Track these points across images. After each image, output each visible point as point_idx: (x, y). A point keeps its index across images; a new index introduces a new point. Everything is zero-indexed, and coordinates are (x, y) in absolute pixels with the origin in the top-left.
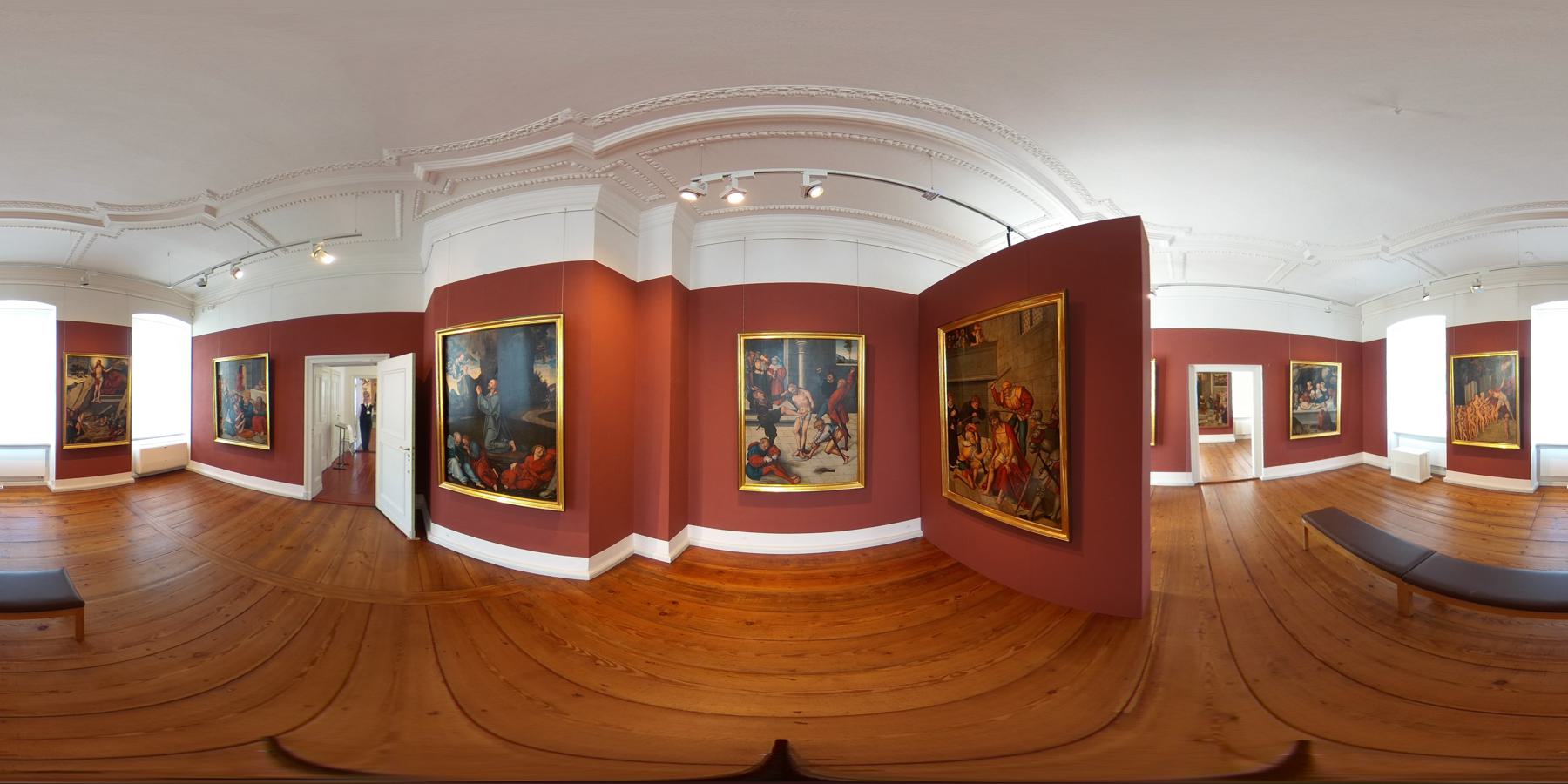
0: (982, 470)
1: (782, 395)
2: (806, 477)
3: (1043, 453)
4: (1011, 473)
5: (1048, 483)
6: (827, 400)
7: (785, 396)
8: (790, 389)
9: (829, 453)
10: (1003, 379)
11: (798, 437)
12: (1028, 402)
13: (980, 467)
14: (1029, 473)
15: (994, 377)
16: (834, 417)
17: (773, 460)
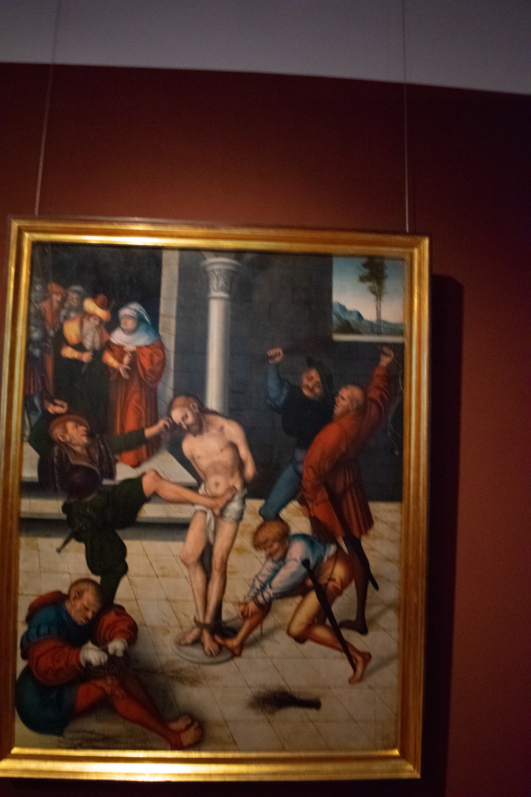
1: (149, 432)
2: (225, 723)
6: (299, 455)
7: (157, 438)
8: (177, 415)
9: (300, 639)
11: (199, 577)
16: (320, 511)
17: (112, 658)
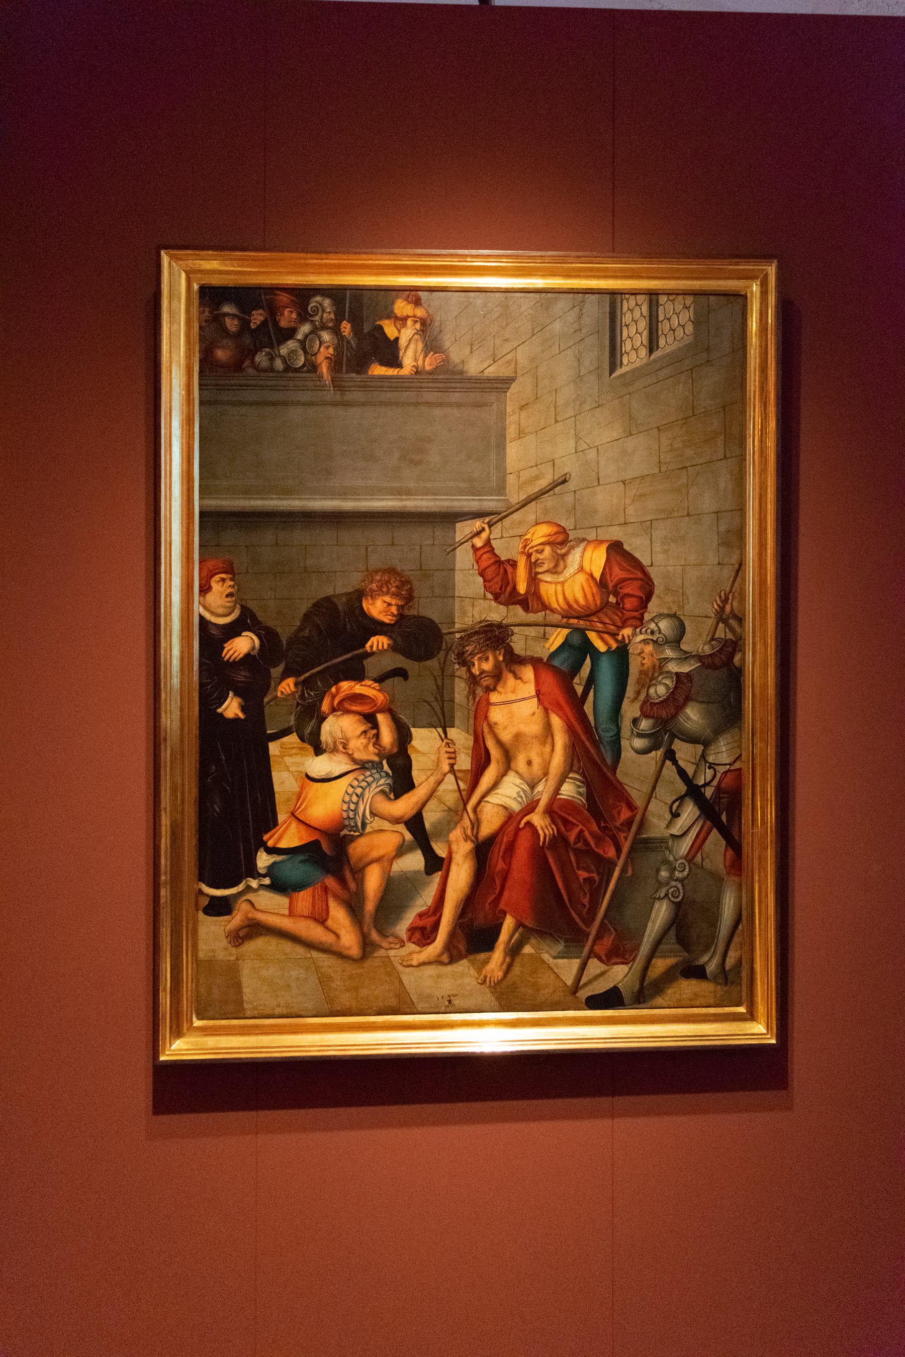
0: (415, 861)
3: (685, 752)
4: (558, 842)
5: (698, 845)
10: (530, 513)
13: (402, 851)
14: (629, 823)
15: (490, 503)
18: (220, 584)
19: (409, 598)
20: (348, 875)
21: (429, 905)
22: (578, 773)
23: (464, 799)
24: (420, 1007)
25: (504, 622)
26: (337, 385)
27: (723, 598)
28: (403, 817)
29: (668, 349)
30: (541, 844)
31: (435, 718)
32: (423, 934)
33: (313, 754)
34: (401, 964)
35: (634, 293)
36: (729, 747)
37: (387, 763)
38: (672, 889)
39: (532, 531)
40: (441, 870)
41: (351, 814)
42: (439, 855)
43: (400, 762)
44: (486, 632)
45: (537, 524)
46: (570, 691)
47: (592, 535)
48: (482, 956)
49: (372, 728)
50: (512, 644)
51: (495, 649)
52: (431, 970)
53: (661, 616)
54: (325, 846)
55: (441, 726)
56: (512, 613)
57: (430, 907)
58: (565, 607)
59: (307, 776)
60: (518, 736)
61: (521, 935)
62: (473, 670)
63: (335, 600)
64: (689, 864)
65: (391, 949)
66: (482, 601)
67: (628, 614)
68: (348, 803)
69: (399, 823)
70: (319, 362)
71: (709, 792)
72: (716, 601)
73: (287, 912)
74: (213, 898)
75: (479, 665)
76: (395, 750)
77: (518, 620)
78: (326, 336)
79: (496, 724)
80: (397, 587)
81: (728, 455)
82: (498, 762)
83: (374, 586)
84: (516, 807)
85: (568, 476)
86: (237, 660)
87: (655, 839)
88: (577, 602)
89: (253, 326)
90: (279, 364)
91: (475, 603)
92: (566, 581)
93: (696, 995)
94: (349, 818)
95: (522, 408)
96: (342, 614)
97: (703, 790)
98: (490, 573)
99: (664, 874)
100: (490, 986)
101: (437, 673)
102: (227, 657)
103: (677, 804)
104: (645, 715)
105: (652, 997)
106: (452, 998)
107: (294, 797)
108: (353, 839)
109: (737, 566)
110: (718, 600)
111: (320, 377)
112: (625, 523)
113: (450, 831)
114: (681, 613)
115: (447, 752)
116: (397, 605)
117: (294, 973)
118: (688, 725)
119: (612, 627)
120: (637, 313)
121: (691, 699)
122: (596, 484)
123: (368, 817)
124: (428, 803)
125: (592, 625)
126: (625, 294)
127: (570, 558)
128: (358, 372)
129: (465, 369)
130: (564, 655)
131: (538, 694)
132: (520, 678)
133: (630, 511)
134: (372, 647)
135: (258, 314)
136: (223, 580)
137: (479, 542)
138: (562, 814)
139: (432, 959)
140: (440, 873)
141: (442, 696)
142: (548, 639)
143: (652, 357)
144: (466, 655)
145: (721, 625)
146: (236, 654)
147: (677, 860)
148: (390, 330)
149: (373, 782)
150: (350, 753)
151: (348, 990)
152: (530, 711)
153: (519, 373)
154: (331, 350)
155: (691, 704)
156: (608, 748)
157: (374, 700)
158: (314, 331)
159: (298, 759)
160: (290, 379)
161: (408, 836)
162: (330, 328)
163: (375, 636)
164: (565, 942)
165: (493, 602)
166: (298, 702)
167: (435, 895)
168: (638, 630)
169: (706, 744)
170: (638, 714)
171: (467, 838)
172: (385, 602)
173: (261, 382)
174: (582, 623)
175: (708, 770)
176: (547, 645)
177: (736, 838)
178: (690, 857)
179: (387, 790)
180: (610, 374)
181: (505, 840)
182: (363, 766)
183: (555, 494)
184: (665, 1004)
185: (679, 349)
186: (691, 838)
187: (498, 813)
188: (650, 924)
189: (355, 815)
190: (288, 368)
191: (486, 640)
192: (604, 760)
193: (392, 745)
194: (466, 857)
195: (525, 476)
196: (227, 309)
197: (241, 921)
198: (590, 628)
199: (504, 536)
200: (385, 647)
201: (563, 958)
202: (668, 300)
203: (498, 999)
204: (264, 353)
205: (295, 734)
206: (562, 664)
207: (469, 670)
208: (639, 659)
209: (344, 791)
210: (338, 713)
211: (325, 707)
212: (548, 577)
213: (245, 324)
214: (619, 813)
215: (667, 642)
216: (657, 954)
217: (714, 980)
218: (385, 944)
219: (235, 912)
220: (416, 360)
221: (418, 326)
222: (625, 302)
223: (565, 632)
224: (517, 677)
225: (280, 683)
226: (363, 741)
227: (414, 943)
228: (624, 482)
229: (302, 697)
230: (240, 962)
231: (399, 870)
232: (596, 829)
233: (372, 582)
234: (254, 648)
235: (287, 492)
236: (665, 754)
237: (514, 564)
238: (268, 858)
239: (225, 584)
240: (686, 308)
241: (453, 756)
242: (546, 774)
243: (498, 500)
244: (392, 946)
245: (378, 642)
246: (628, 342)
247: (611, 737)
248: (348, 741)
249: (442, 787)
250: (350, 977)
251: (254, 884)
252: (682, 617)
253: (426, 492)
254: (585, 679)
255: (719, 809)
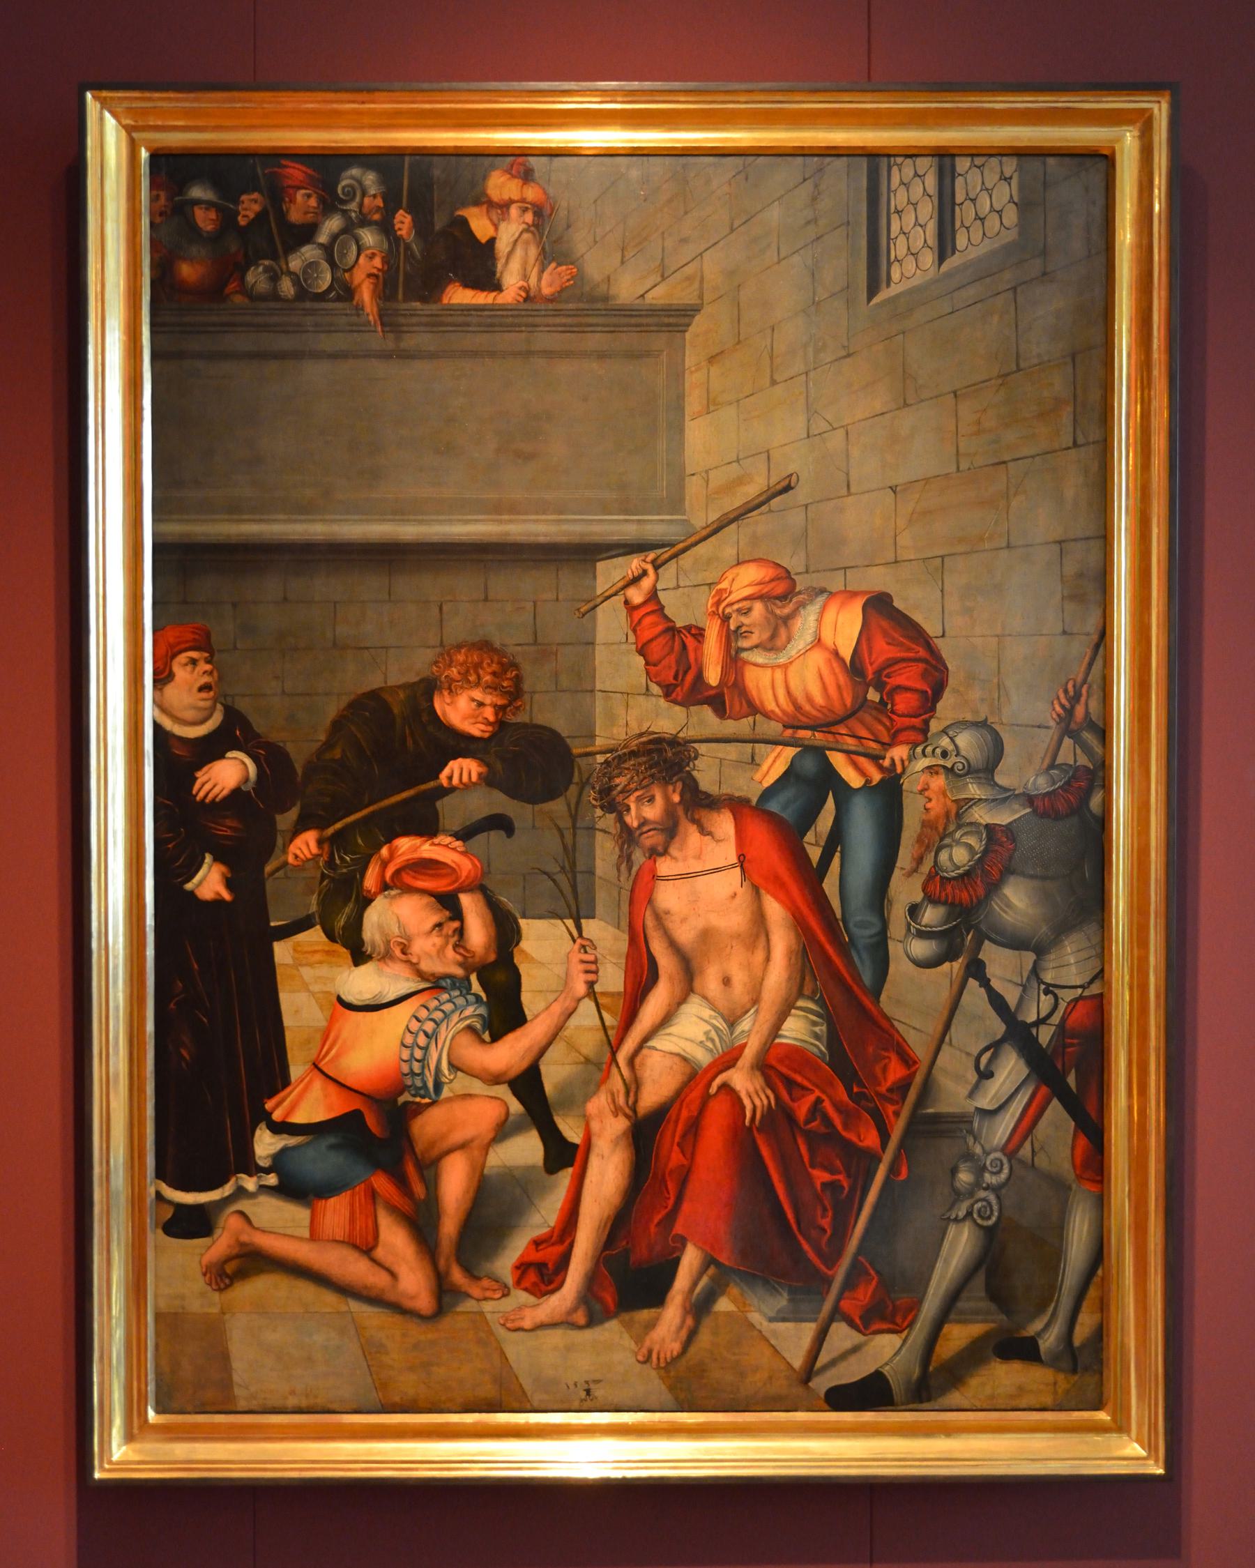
5: (1027, 1127)
10: (726, 545)
12: (908, 677)
14: (902, 1088)
15: (655, 527)
18: (189, 668)
19: (515, 694)
20: (410, 1169)
21: (552, 1224)
22: (811, 998)
23: (613, 1042)
24: (536, 1399)
25: (681, 735)
26: (389, 321)
27: (1071, 693)
28: (505, 1073)
29: (973, 254)
30: (747, 1122)
31: (562, 902)
32: (542, 1275)
33: (351, 963)
34: (504, 1325)
35: (912, 154)
36: (1084, 955)
37: (479, 978)
38: (979, 1205)
39: (730, 575)
40: (572, 1165)
41: (416, 1067)
42: (570, 1140)
43: (500, 977)
44: (650, 752)
45: (738, 564)
46: (797, 855)
47: (836, 583)
48: (645, 1314)
49: (452, 919)
50: (695, 773)
51: (666, 782)
52: (556, 1337)
53: (963, 724)
54: (371, 1121)
55: (571, 917)
56: (694, 719)
57: (554, 1228)
58: (789, 708)
59: (340, 999)
60: (706, 935)
61: (712, 1279)
62: (628, 819)
63: (386, 696)
64: (1010, 1161)
65: (485, 1299)
66: (641, 699)
67: (900, 722)
68: (411, 1047)
69: (498, 1083)
70: (356, 282)
71: (1045, 1036)
72: (1058, 698)
73: (306, 1233)
74: (179, 1207)
75: (638, 809)
76: (492, 957)
77: (707, 732)
78: (369, 237)
79: (667, 913)
80: (494, 674)
81: (1080, 440)
82: (671, 978)
83: (454, 672)
84: (703, 1058)
85: (794, 478)
86: (217, 800)
87: (953, 1115)
88: (809, 699)
89: (242, 222)
90: (287, 287)
91: (631, 702)
92: (791, 663)
93: (1021, 1390)
94: (412, 1073)
95: (712, 360)
96: (399, 721)
97: (1034, 1031)
98: (656, 649)
99: (965, 1177)
100: (658, 1367)
101: (565, 823)
102: (201, 794)
103: (988, 1055)
104: (931, 899)
105: (944, 1390)
106: (592, 1386)
107: (318, 1037)
108: (419, 1110)
109: (1095, 637)
110: (1062, 696)
111: (359, 308)
112: (896, 562)
113: (587, 1098)
114: (997, 720)
115: (583, 962)
116: (495, 706)
117: (319, 1338)
118: (1009, 918)
119: (873, 745)
120: (917, 191)
121: (1013, 873)
122: (844, 492)
123: (446, 1072)
124: (551, 1048)
125: (837, 742)
126: (895, 156)
127: (798, 623)
128: (424, 300)
129: (611, 292)
130: (788, 794)
131: (742, 861)
132: (710, 834)
133: (905, 540)
134: (450, 778)
135: (252, 200)
136: (194, 662)
137: (636, 595)
138: (784, 1070)
139: (557, 1319)
140: (570, 1170)
141: (573, 864)
142: (759, 765)
143: (946, 266)
144: (615, 793)
145: (1068, 742)
146: (216, 790)
147: (988, 1154)
148: (480, 225)
149: (453, 1012)
150: (415, 960)
151: (411, 1369)
152: (728, 891)
153: (708, 297)
154: (377, 262)
155: (1012, 879)
156: (865, 956)
157: (453, 869)
158: (348, 229)
159: (324, 971)
160: (312, 312)
161: (516, 1106)
162: (376, 223)
163: (455, 758)
164: (789, 1294)
165: (662, 701)
166: (323, 874)
167: (562, 1209)
168: (919, 749)
169: (1041, 951)
170: (918, 897)
171: (616, 1111)
172: (473, 700)
173: (259, 320)
174: (819, 738)
175: (1043, 997)
176: (758, 776)
177: (1093, 1115)
178: (1011, 1146)
179: (478, 1026)
180: (869, 300)
181: (685, 1114)
182: (436, 984)
183: (770, 511)
184: (966, 1404)
185: (993, 253)
186: (1013, 1115)
187: (671, 1068)
188: (939, 1265)
189: (423, 1068)
190: (303, 293)
191: (651, 767)
192: (857, 978)
193: (487, 949)
194: (616, 1142)
195: (717, 478)
196: (197, 192)
197: (229, 1246)
198: (833, 745)
199: (682, 584)
200: (474, 778)
201: (784, 1320)
202: (973, 165)
203: (671, 1389)
204: (261, 269)
205: (318, 927)
206: (785, 808)
207: (620, 820)
208: (921, 800)
209: (404, 1027)
210: (393, 892)
211: (370, 881)
212: (758, 657)
213: (228, 219)
214: (885, 1069)
215: (970, 771)
216: (952, 1316)
217: (1054, 1362)
218: (475, 1291)
219: (218, 1232)
220: (525, 277)
221: (529, 217)
222: (895, 170)
223: (790, 752)
224: (703, 831)
225: (291, 841)
226: (436, 940)
227: (526, 1290)
228: (893, 489)
229: (330, 863)
230: (227, 1317)
231: (500, 1163)
232: (845, 1098)
233: (450, 666)
234: (247, 780)
235: (304, 509)
236: (968, 967)
237: (698, 633)
238: (273, 1140)
239: (198, 669)
240: (1005, 179)
241: (592, 969)
242: (756, 1001)
243: (671, 521)
244: (488, 1294)
245: (463, 769)
246: (901, 242)
247: (871, 937)
248: (409, 939)
249: (573, 1022)
250: (416, 1346)
251: (250, 1184)
252: (996, 727)
253: (542, 508)
254: (825, 837)
255: (1063, 1065)
